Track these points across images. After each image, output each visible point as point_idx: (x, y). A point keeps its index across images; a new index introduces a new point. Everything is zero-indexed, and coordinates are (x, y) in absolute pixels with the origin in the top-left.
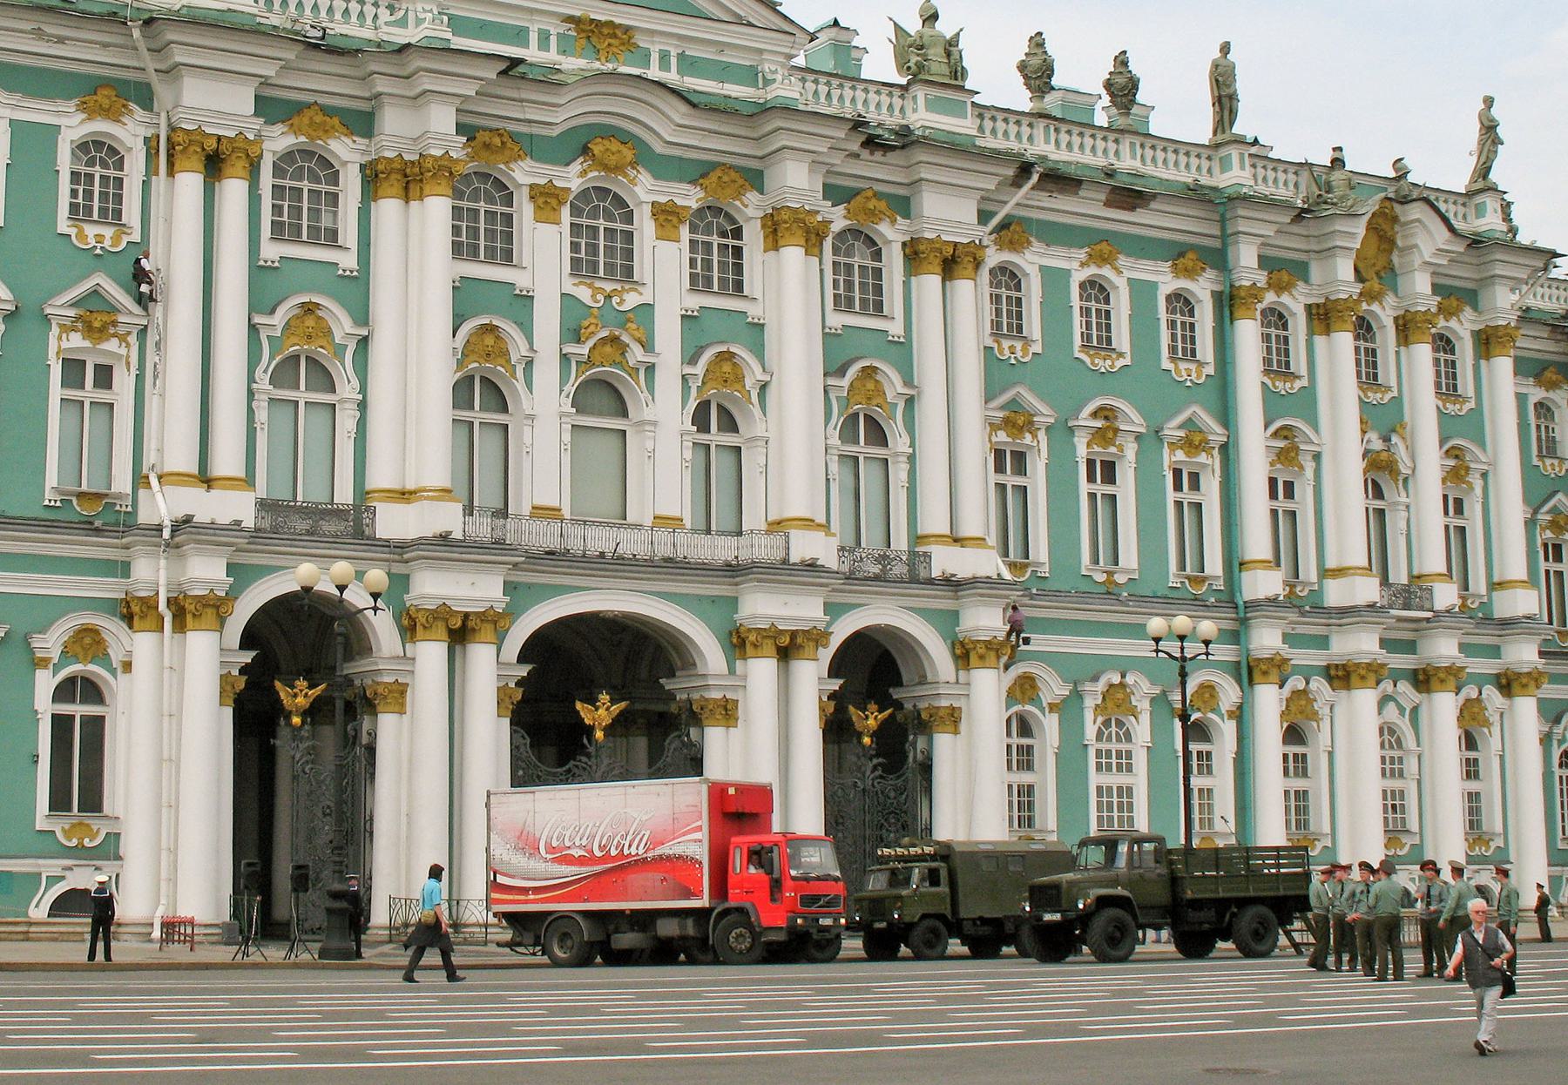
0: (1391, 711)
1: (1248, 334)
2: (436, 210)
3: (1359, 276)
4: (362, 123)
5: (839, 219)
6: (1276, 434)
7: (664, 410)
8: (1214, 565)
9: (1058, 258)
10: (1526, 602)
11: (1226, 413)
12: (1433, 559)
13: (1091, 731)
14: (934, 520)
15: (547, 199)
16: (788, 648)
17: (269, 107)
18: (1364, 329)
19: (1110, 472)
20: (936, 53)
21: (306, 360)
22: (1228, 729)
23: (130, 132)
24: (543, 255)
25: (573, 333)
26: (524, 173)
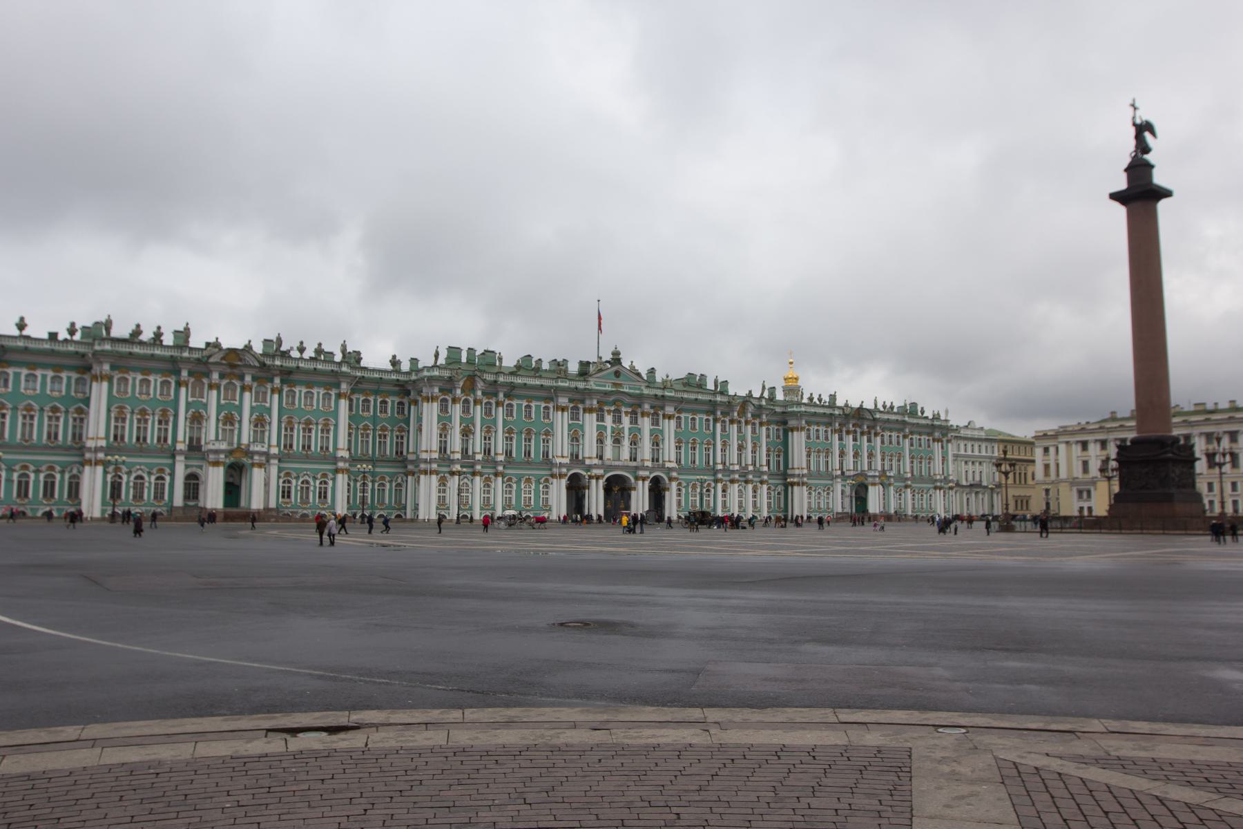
1: (719, 426)
2: (594, 415)
4: (583, 402)
7: (626, 443)
10: (765, 469)
11: (714, 439)
12: (750, 462)
15: (609, 412)
16: (644, 479)
17: (571, 401)
18: (739, 422)
21: (575, 438)
23: (551, 405)
26: (606, 408)
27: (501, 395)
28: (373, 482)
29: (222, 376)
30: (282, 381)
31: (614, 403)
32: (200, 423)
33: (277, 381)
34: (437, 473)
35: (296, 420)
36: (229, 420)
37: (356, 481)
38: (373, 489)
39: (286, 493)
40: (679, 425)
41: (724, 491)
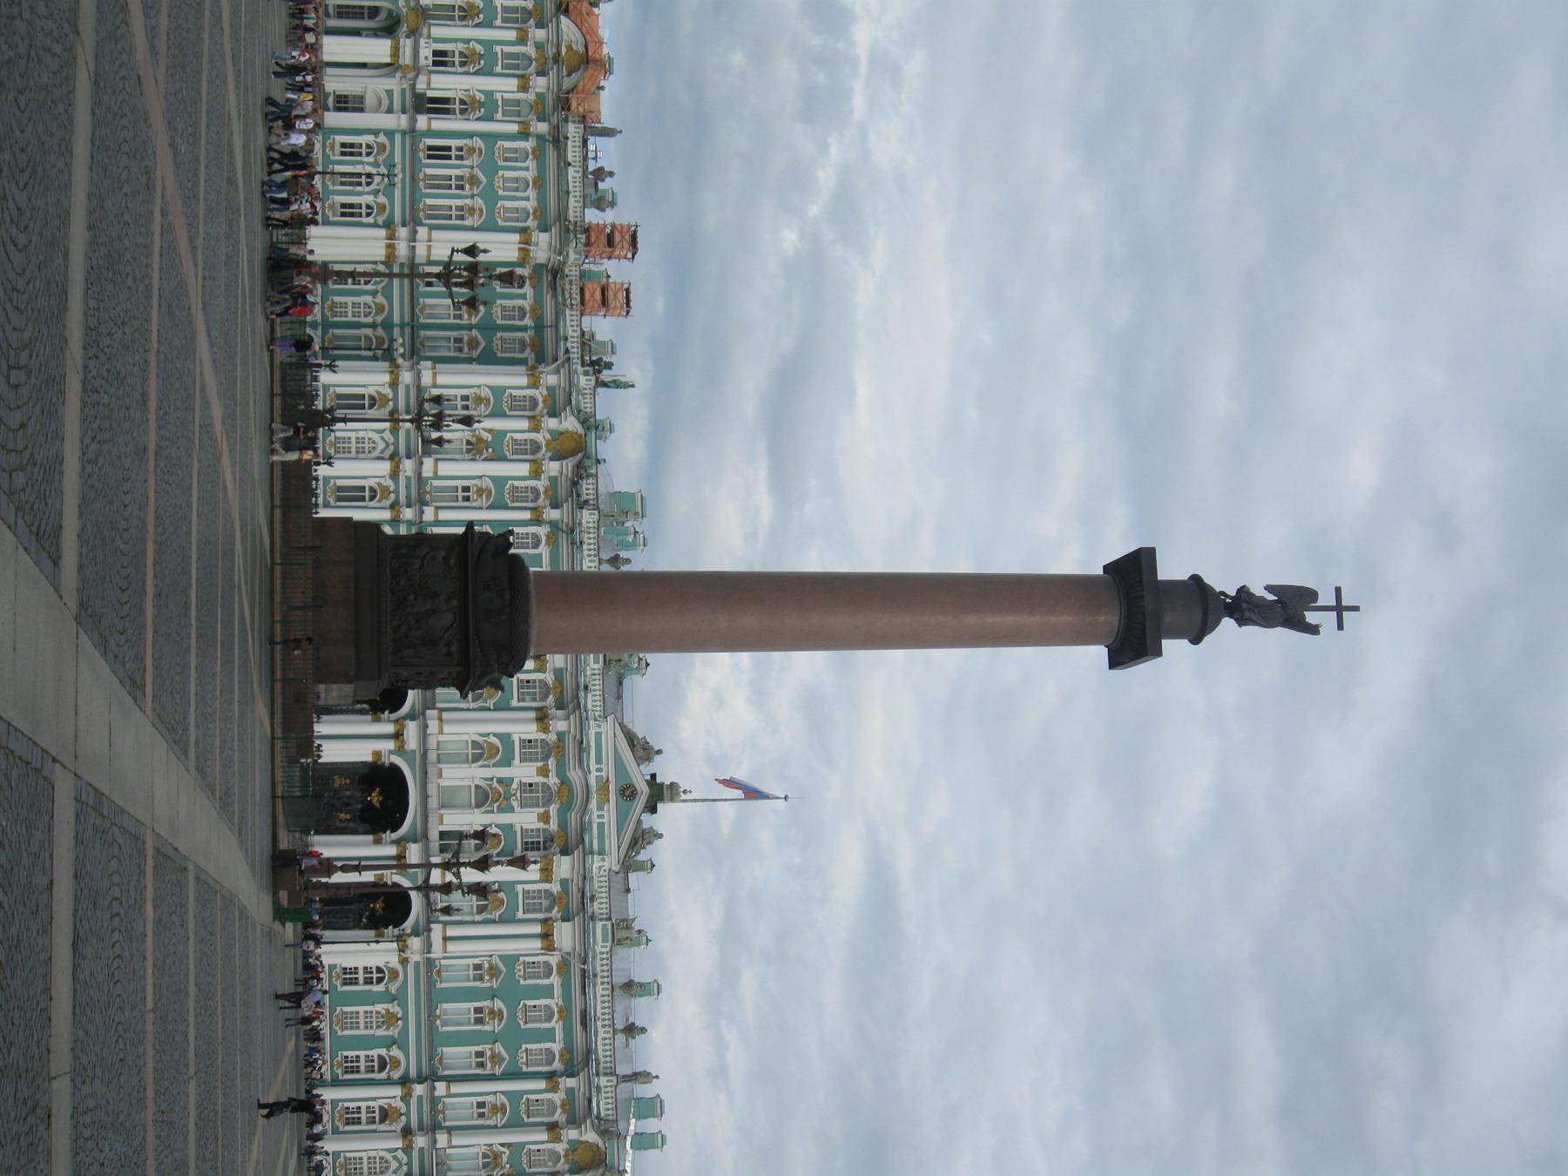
0: (394, 1165)
3: (575, 1146)
4: (560, 705)
5: (555, 888)
6: (503, 1105)
8: (446, 1073)
9: (557, 991)
13: (380, 1007)
14: (451, 932)
15: (544, 772)
19: (479, 1021)
20: (625, 934)
22: (383, 1075)
24: (523, 772)
25: (500, 781)
26: (551, 762)
27: (554, 514)
28: (374, 326)
29: (539, 46)
30: (540, 138)
31: (564, 781)
32: (462, 18)
33: (542, 128)
34: (394, 384)
35: (474, 160)
36: (467, 59)
37: (374, 293)
38: (358, 325)
39: (349, 150)
40: (532, 969)
41: (385, 1115)
